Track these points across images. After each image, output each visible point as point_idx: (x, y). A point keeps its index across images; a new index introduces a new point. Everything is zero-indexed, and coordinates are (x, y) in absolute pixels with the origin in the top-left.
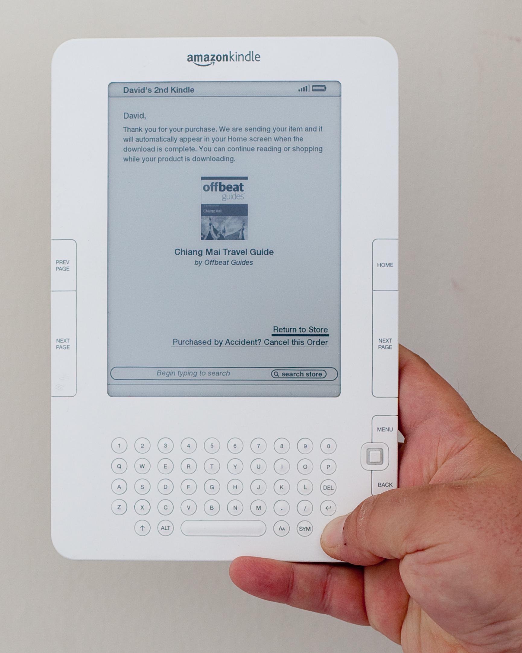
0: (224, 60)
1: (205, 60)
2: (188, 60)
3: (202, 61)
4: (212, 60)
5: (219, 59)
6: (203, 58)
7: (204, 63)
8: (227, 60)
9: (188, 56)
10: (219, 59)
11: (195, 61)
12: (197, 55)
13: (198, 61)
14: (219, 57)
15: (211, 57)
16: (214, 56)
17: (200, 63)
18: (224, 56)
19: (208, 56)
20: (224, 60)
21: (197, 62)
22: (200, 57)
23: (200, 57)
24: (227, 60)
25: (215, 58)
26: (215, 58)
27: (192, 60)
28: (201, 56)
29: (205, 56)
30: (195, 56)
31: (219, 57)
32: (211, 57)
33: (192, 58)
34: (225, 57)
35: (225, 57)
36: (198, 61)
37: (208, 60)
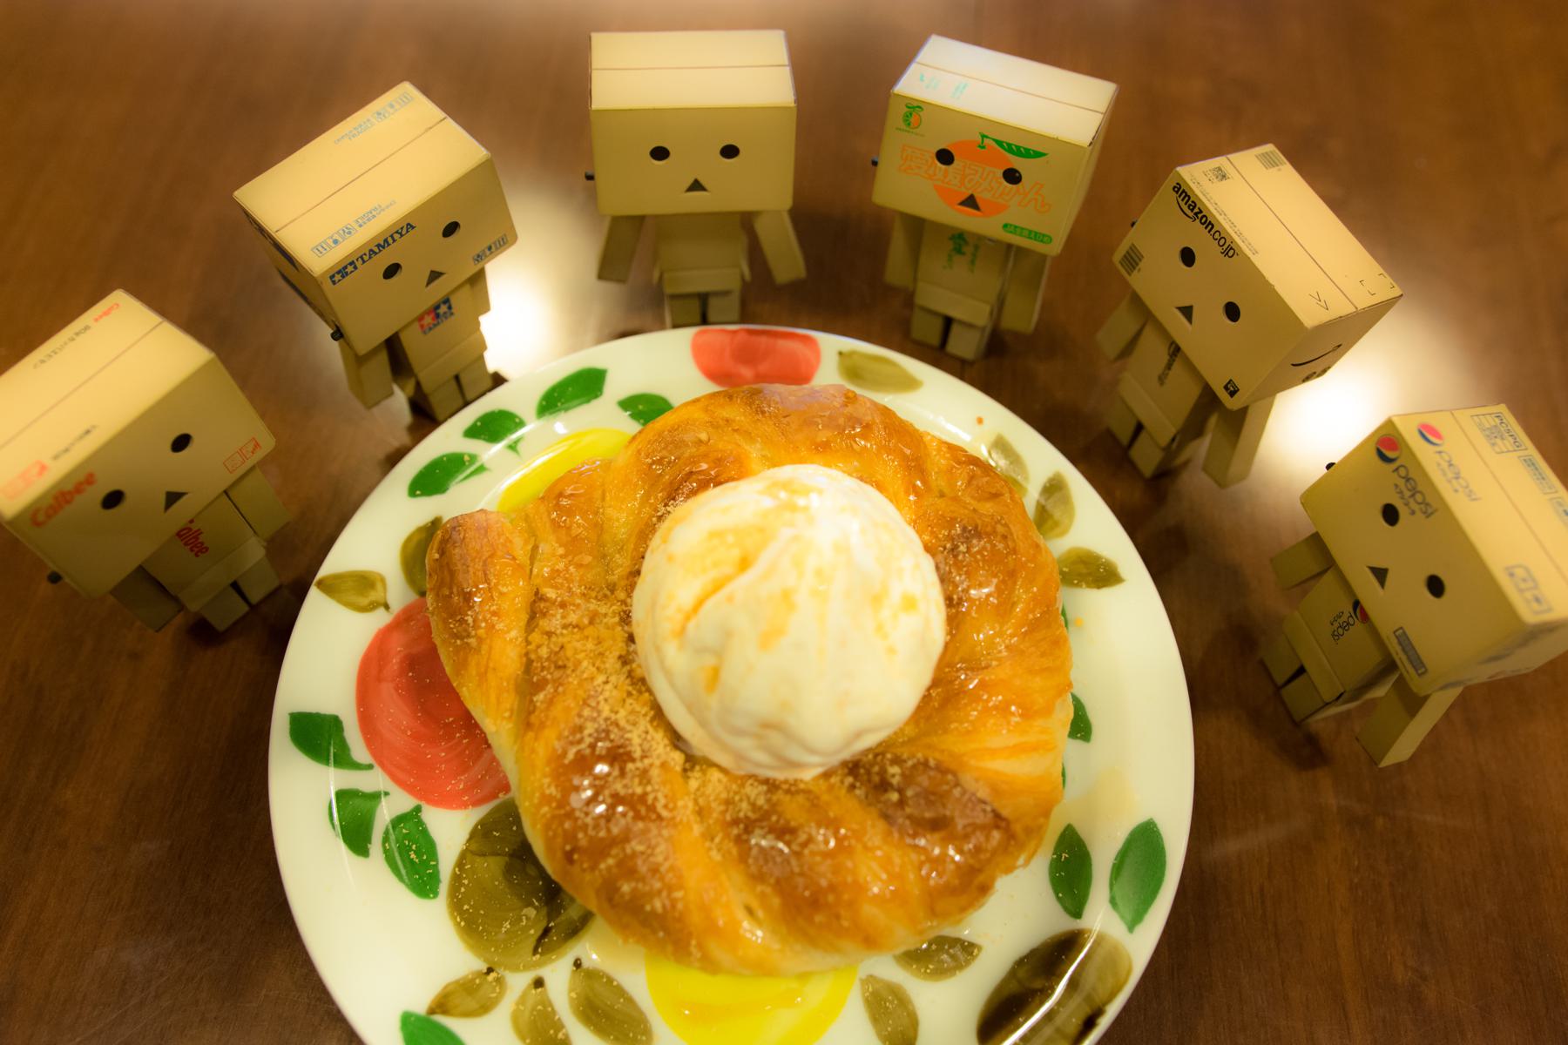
0: (1206, 228)
1: (1189, 207)
2: (1175, 187)
3: (1186, 204)
4: (1196, 214)
5: (1203, 221)
6: (1190, 202)
7: (1185, 208)
8: (1209, 232)
9: (1178, 184)
10: (1203, 221)
11: (1180, 196)
12: (1186, 193)
13: (1183, 200)
14: (1204, 220)
15: (1196, 210)
16: (1201, 212)
17: (1182, 204)
18: (1210, 223)
19: (1196, 205)
20: (1206, 228)
21: (1180, 200)
22: (1187, 198)
23: (1187, 198)
24: (1209, 232)
25: (1200, 216)
26: (1200, 216)
27: (1177, 192)
28: (1189, 198)
29: (1193, 202)
30: (1184, 191)
31: (1204, 220)
32: (1196, 210)
33: (1179, 189)
34: (1210, 226)
35: (1210, 226)
36: (1183, 200)
37: (1192, 210)
